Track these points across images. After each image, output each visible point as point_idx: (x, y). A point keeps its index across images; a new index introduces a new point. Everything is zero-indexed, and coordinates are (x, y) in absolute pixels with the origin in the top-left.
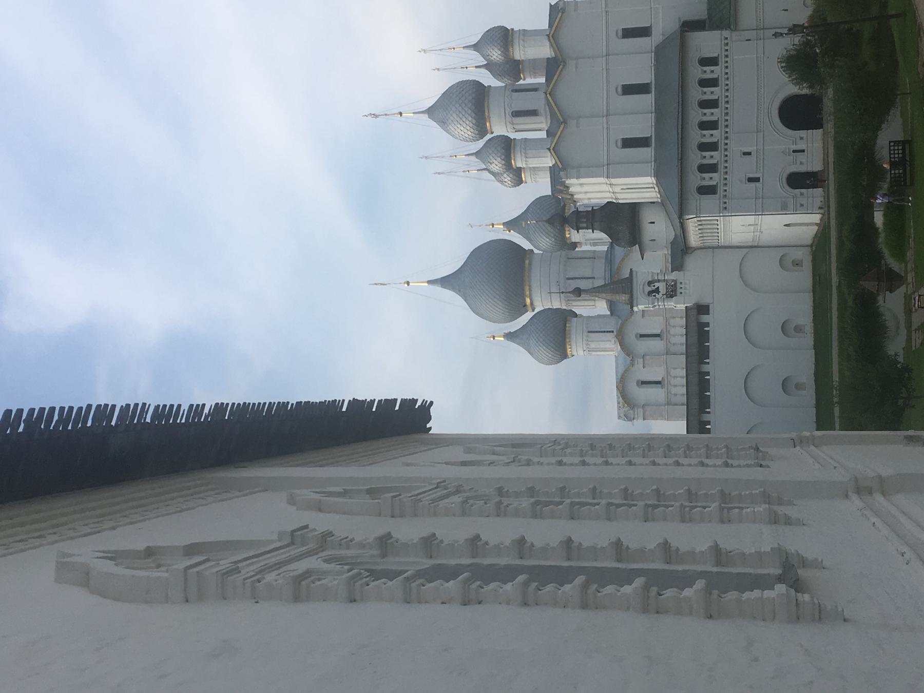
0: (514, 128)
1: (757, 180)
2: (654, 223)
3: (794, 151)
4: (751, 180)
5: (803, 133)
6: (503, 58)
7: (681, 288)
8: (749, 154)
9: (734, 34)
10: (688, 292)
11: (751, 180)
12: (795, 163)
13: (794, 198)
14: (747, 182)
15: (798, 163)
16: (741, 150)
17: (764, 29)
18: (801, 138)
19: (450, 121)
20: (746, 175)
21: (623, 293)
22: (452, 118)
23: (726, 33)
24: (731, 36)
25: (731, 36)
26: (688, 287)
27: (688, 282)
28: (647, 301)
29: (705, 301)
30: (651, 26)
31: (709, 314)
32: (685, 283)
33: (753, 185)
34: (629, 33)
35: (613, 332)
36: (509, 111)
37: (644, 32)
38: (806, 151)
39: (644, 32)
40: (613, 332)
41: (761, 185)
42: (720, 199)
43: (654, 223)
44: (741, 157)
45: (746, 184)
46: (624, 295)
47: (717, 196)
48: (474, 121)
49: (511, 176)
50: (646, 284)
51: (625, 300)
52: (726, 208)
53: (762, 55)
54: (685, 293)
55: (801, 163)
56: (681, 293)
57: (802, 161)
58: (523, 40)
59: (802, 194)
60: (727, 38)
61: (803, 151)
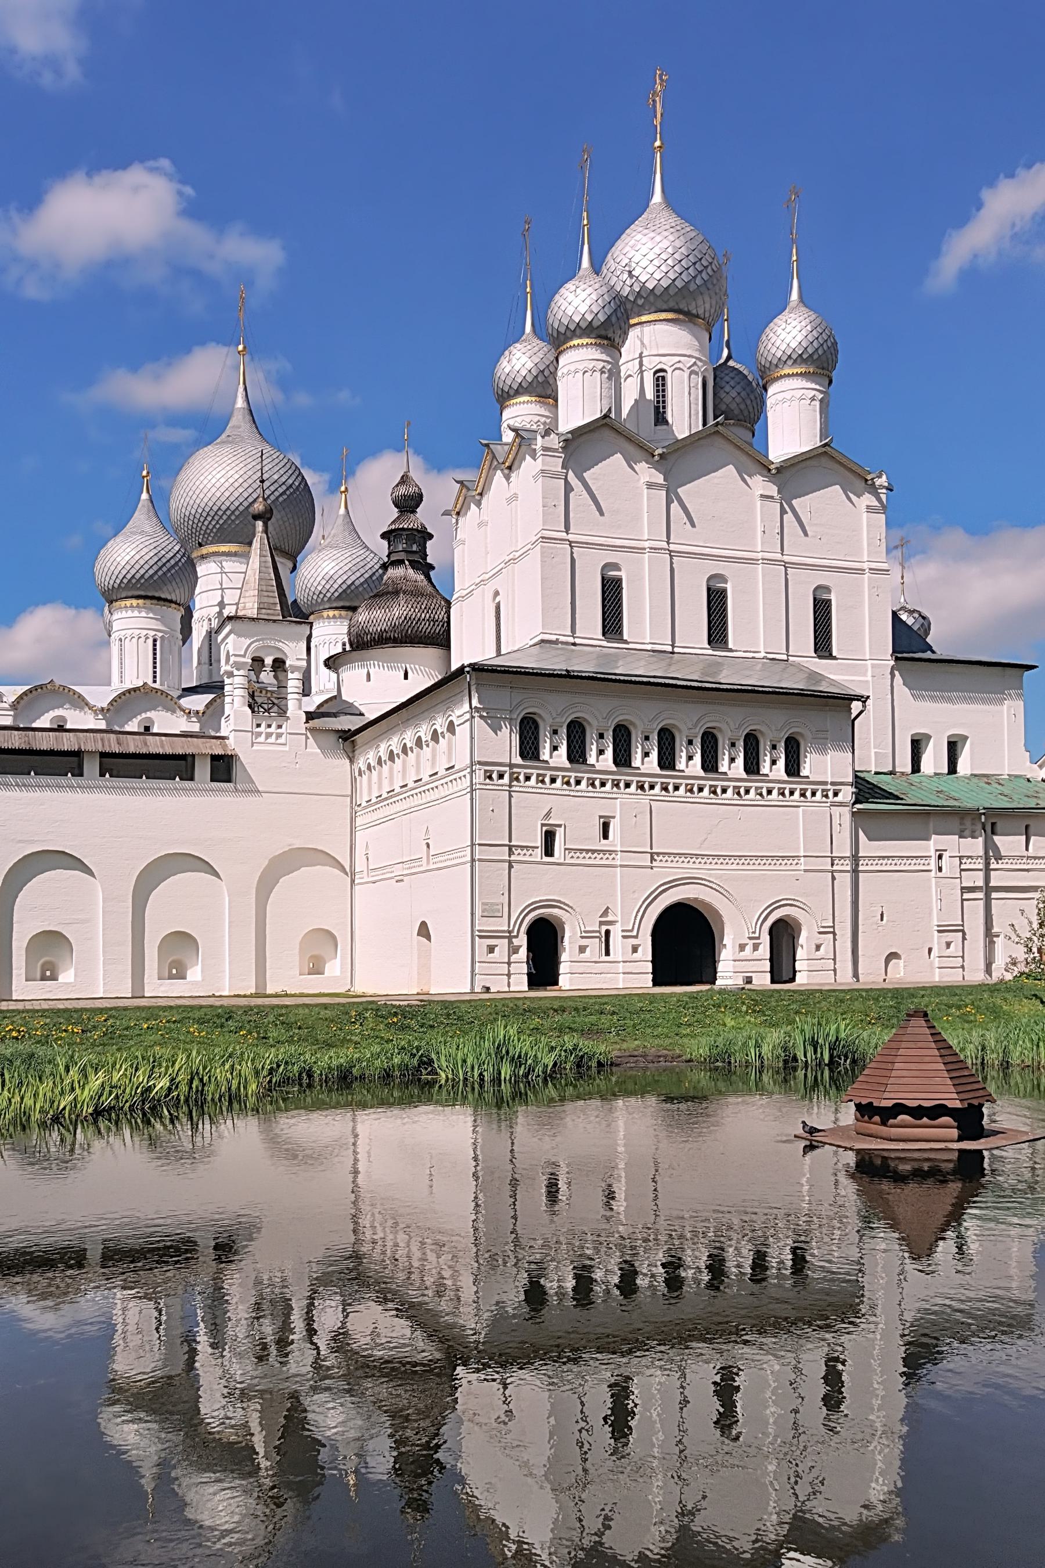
0: (630, 376)
1: (549, 851)
2: (406, 677)
3: (608, 932)
4: (549, 837)
5: (646, 952)
6: (779, 354)
7: (269, 726)
8: (606, 836)
9: (846, 811)
10: (262, 739)
11: (549, 837)
12: (584, 934)
13: (510, 932)
14: (544, 829)
15: (584, 942)
16: (614, 817)
17: (855, 872)
18: (635, 949)
19: (652, 235)
20: (560, 826)
21: (259, 603)
22: (658, 238)
23: (847, 794)
24: (841, 804)
25: (841, 804)
26: (272, 739)
27: (282, 740)
28: (242, 653)
29: (237, 772)
30: (835, 658)
31: (212, 781)
32: (279, 736)
33: (539, 841)
34: (822, 610)
35: (155, 682)
36: (667, 363)
37: (823, 645)
38: (607, 959)
39: (823, 645)
40: (155, 682)
41: (539, 859)
42: (511, 766)
43: (406, 677)
44: (601, 817)
45: (543, 825)
46: (256, 606)
47: (518, 760)
48: (650, 285)
49: (524, 372)
50: (279, 656)
51: (244, 608)
52: (490, 778)
53: (802, 867)
54: (259, 734)
55: (582, 949)
56: (259, 726)
57: (588, 949)
58: (813, 399)
59: (516, 950)
60: (836, 794)
61: (607, 953)
